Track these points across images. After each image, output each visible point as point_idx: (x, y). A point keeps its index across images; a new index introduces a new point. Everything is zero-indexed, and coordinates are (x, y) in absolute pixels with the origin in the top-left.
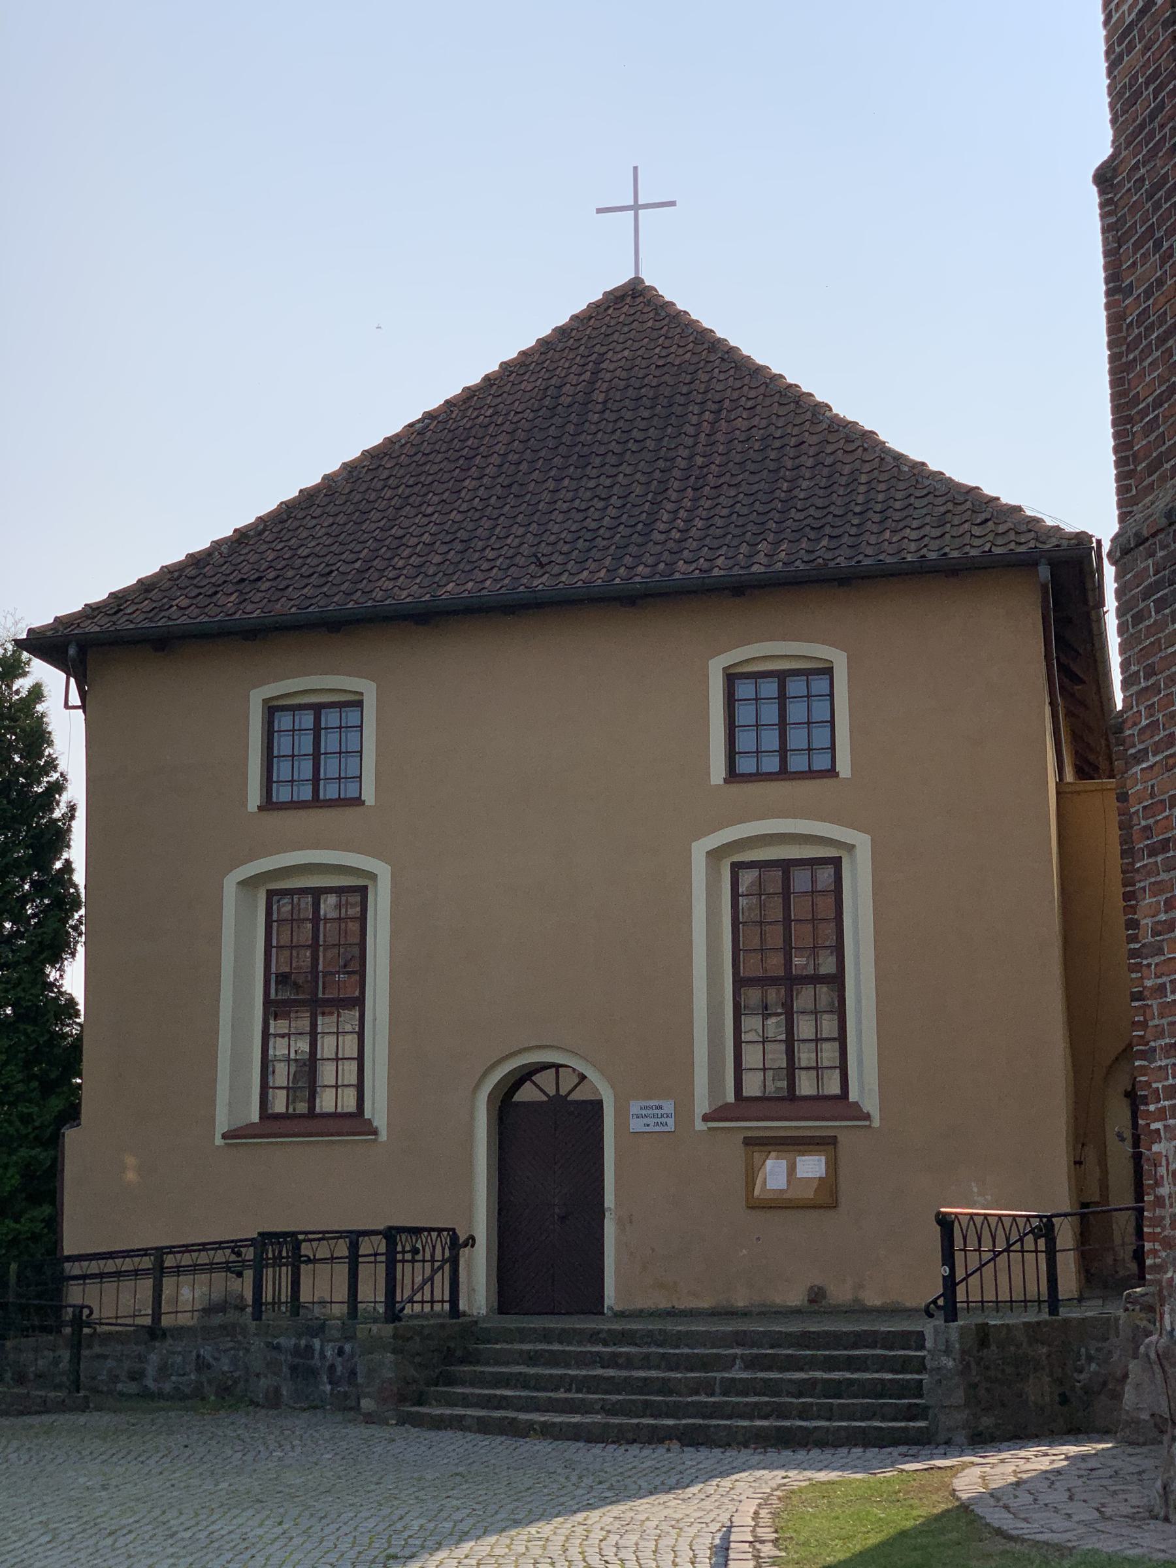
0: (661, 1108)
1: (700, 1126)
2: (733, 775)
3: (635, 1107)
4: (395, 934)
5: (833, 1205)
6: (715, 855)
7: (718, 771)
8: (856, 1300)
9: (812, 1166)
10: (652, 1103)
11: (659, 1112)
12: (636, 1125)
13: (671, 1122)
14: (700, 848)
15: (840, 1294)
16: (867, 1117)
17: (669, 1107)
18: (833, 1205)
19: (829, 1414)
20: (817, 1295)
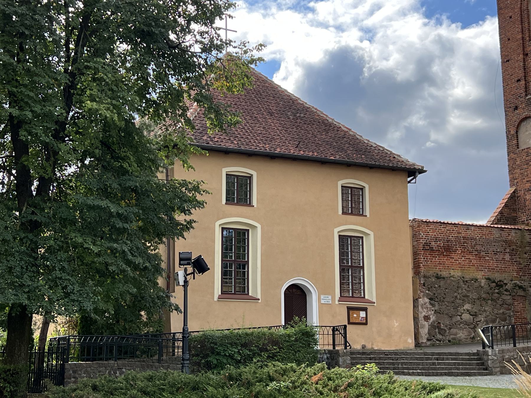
0: (328, 297)
1: (337, 303)
2: (344, 213)
3: (322, 297)
4: (262, 245)
5: (366, 324)
6: (339, 232)
7: (340, 212)
8: (372, 348)
9: (363, 314)
10: (326, 296)
11: (328, 298)
12: (323, 302)
13: (330, 301)
14: (336, 230)
15: (369, 346)
16: (374, 303)
17: (330, 297)
18: (366, 324)
19: (458, 369)
20: (364, 347)
